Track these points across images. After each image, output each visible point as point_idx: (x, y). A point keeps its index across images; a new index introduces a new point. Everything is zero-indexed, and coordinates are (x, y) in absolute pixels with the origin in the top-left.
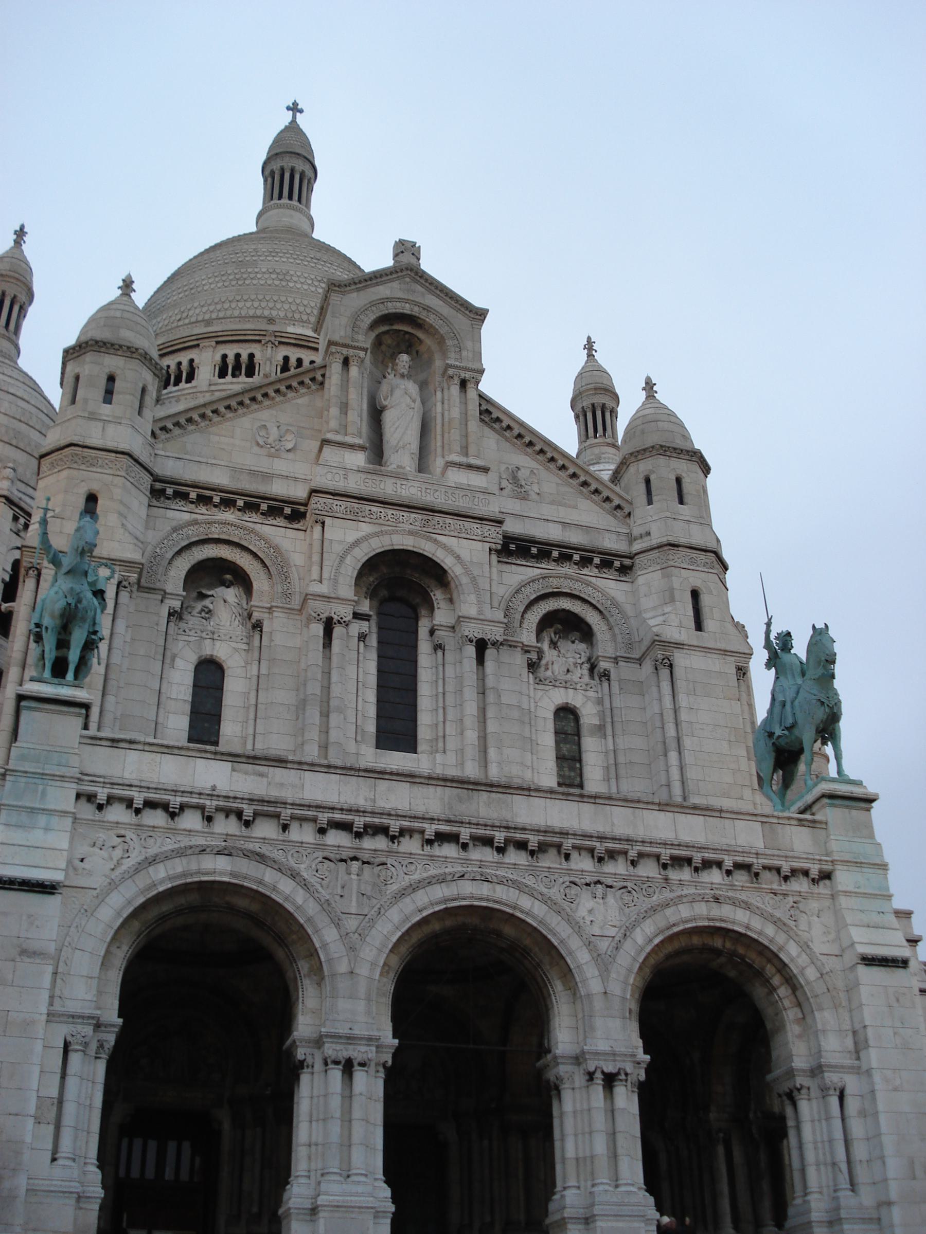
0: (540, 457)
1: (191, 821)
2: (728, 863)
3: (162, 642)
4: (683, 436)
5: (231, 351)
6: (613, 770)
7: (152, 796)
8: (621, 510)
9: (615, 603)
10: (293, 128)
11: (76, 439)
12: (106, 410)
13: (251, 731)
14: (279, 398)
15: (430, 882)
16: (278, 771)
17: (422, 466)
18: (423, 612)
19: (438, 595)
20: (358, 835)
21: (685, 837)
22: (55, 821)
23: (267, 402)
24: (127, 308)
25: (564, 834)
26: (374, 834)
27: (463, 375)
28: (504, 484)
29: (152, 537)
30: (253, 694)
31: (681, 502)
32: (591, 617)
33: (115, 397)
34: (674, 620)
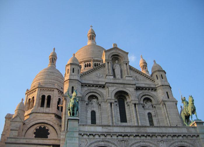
0: (139, 74)
1: (97, 137)
2: (182, 135)
3: (85, 109)
5: (86, 63)
6: (158, 122)
7: (90, 133)
10: (92, 30)
12: (73, 74)
13: (101, 121)
14: (99, 69)
15: (135, 143)
16: (109, 127)
17: (122, 77)
18: (125, 100)
19: (127, 97)
20: (123, 137)
22: (76, 138)
23: (97, 70)
25: (156, 133)
26: (125, 136)
27: (127, 63)
29: (82, 92)
30: (100, 116)
31: (162, 78)
32: (151, 98)
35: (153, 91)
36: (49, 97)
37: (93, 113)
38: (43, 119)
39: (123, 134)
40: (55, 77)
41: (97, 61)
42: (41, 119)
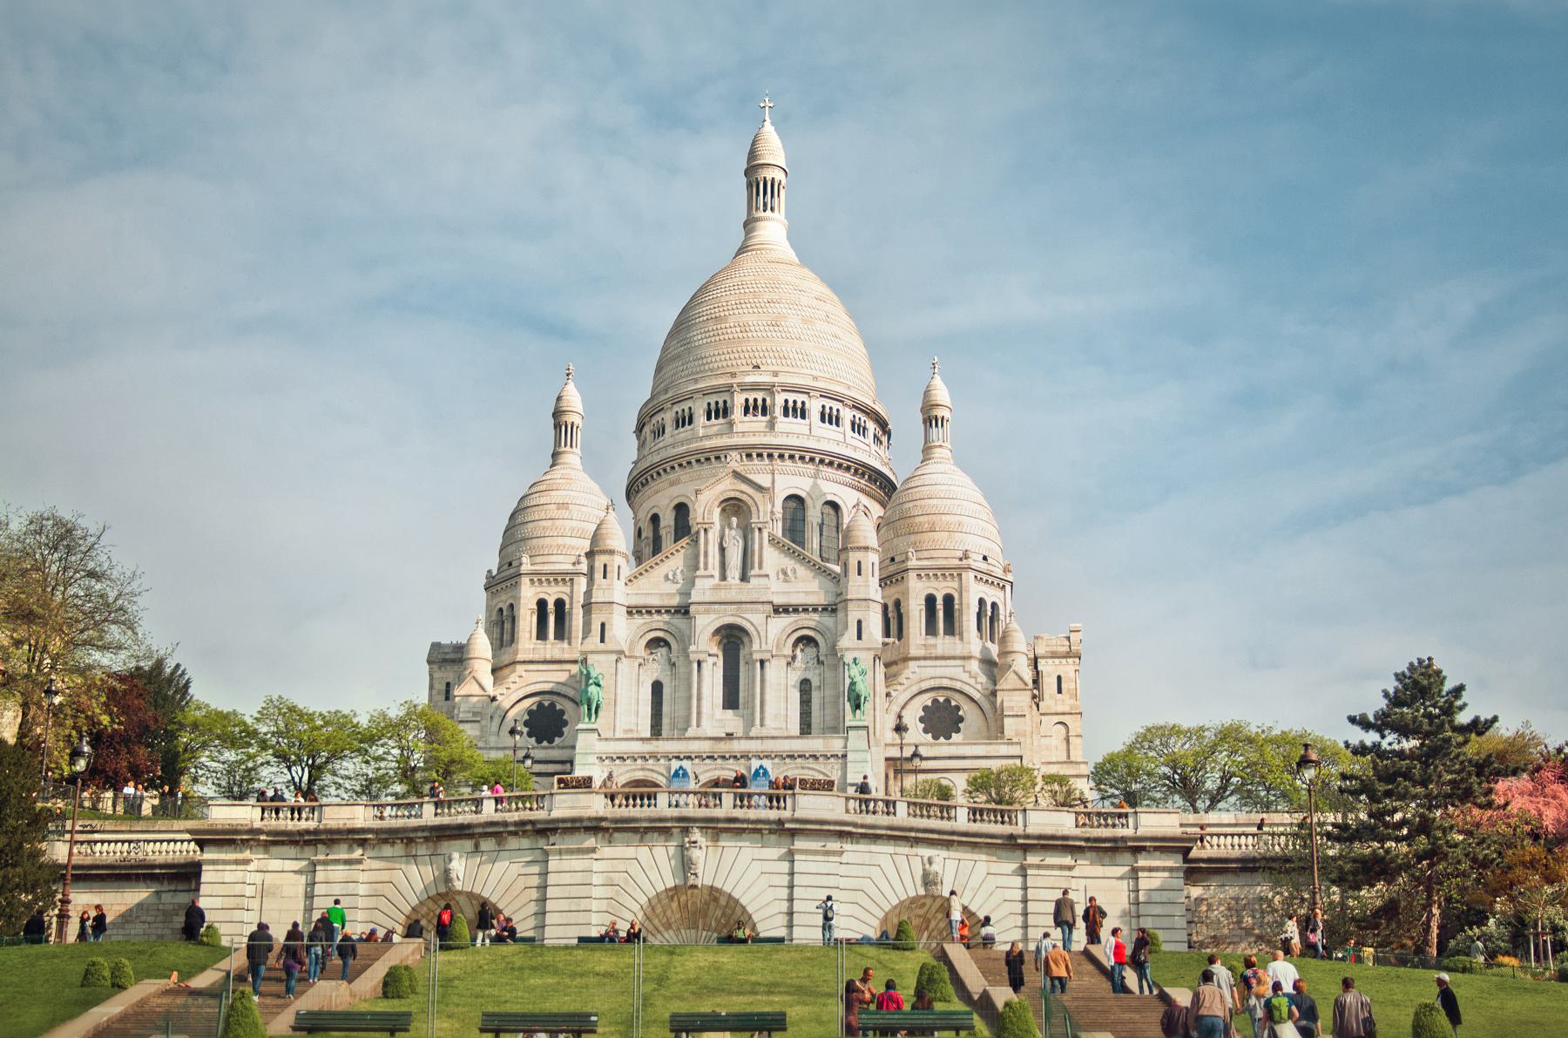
2: (807, 755)
4: (865, 537)
5: (712, 399)
6: (823, 706)
8: (835, 578)
9: (828, 629)
11: (593, 600)
18: (741, 647)
19: (746, 640)
21: (794, 748)
24: (609, 526)
27: (759, 526)
28: (781, 576)
31: (859, 574)
32: (818, 638)
33: (608, 575)
34: (846, 636)
35: (825, 614)
36: (560, 604)
37: (657, 688)
38: (542, 679)
39: (682, 756)
40: (574, 524)
41: (755, 387)
42: (539, 680)
